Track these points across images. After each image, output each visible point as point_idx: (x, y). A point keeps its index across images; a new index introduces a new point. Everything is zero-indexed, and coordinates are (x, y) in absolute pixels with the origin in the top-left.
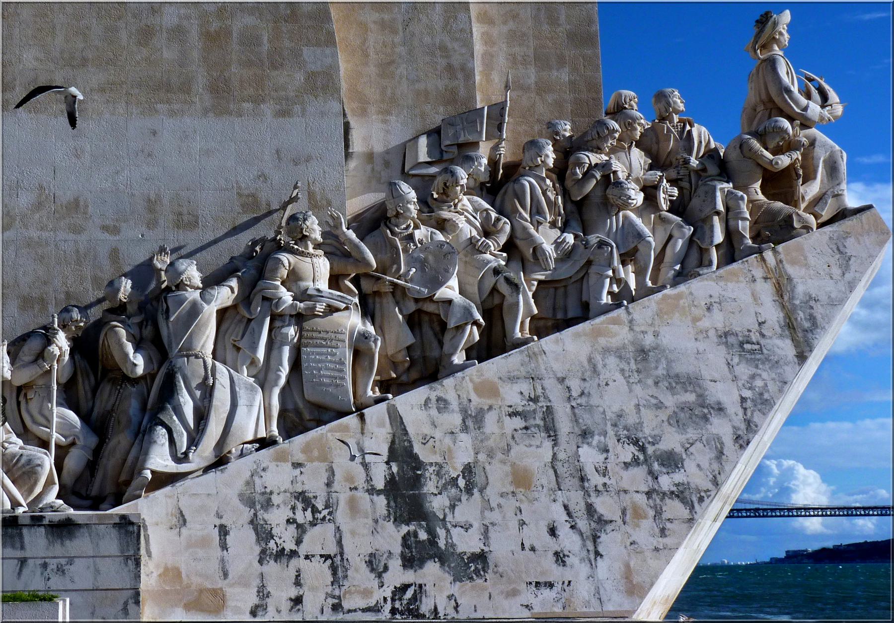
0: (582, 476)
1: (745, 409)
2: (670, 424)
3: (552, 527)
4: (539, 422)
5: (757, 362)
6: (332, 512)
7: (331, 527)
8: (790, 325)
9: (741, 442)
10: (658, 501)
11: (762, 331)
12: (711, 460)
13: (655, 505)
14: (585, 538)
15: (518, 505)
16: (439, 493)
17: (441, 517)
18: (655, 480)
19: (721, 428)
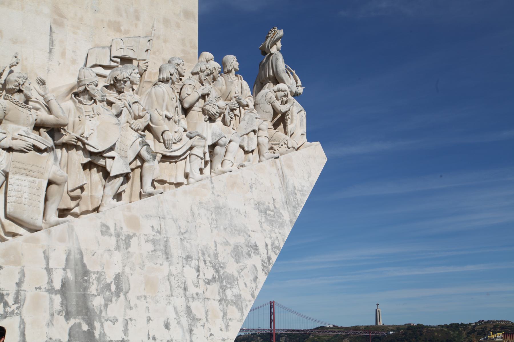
0: (185, 287)
1: (267, 251)
2: (232, 256)
3: (166, 322)
4: (162, 247)
5: (272, 222)
6: (20, 307)
7: (17, 319)
8: (287, 203)
9: (266, 271)
10: (225, 306)
11: (275, 204)
12: (251, 281)
13: (224, 309)
14: (185, 331)
15: (147, 305)
16: (98, 295)
17: (98, 312)
18: (224, 293)
19: (256, 261)
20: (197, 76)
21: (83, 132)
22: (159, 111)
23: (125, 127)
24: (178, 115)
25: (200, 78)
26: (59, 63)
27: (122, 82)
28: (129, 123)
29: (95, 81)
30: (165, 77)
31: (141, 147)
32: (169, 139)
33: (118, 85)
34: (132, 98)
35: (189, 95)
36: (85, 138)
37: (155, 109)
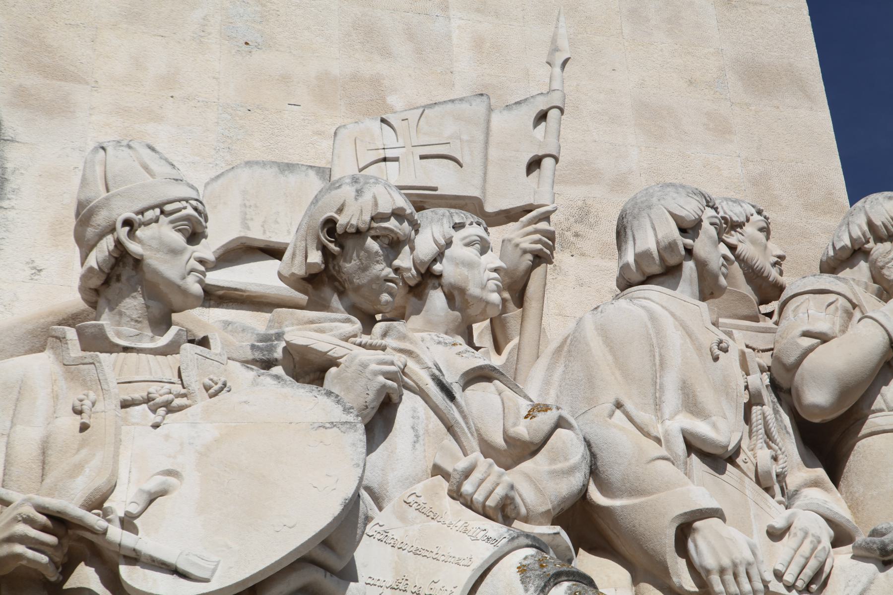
20: (856, 268)
21: (100, 482)
22: (645, 416)
23: (421, 500)
24: (769, 447)
25: (882, 275)
26: (34, 268)
27: (372, 244)
28: (446, 476)
29: (179, 200)
30: (653, 247)
31: (532, 589)
32: (735, 565)
33: (349, 266)
34: (459, 354)
35: (824, 338)
36: (118, 522)
37: (609, 406)
